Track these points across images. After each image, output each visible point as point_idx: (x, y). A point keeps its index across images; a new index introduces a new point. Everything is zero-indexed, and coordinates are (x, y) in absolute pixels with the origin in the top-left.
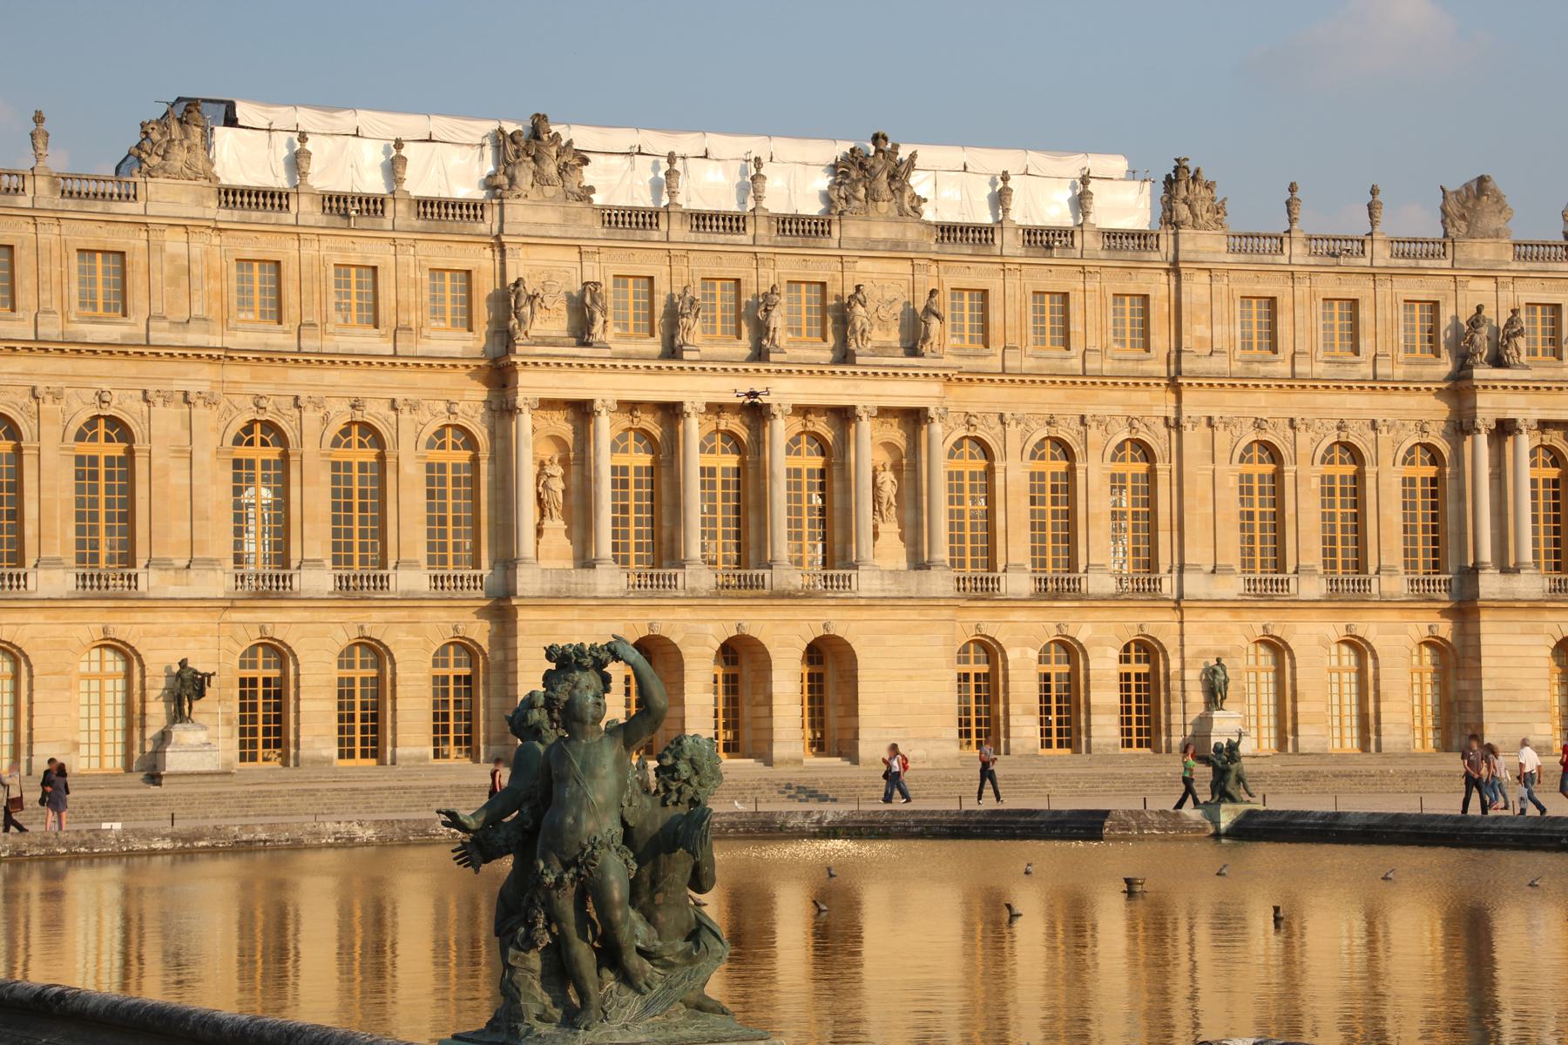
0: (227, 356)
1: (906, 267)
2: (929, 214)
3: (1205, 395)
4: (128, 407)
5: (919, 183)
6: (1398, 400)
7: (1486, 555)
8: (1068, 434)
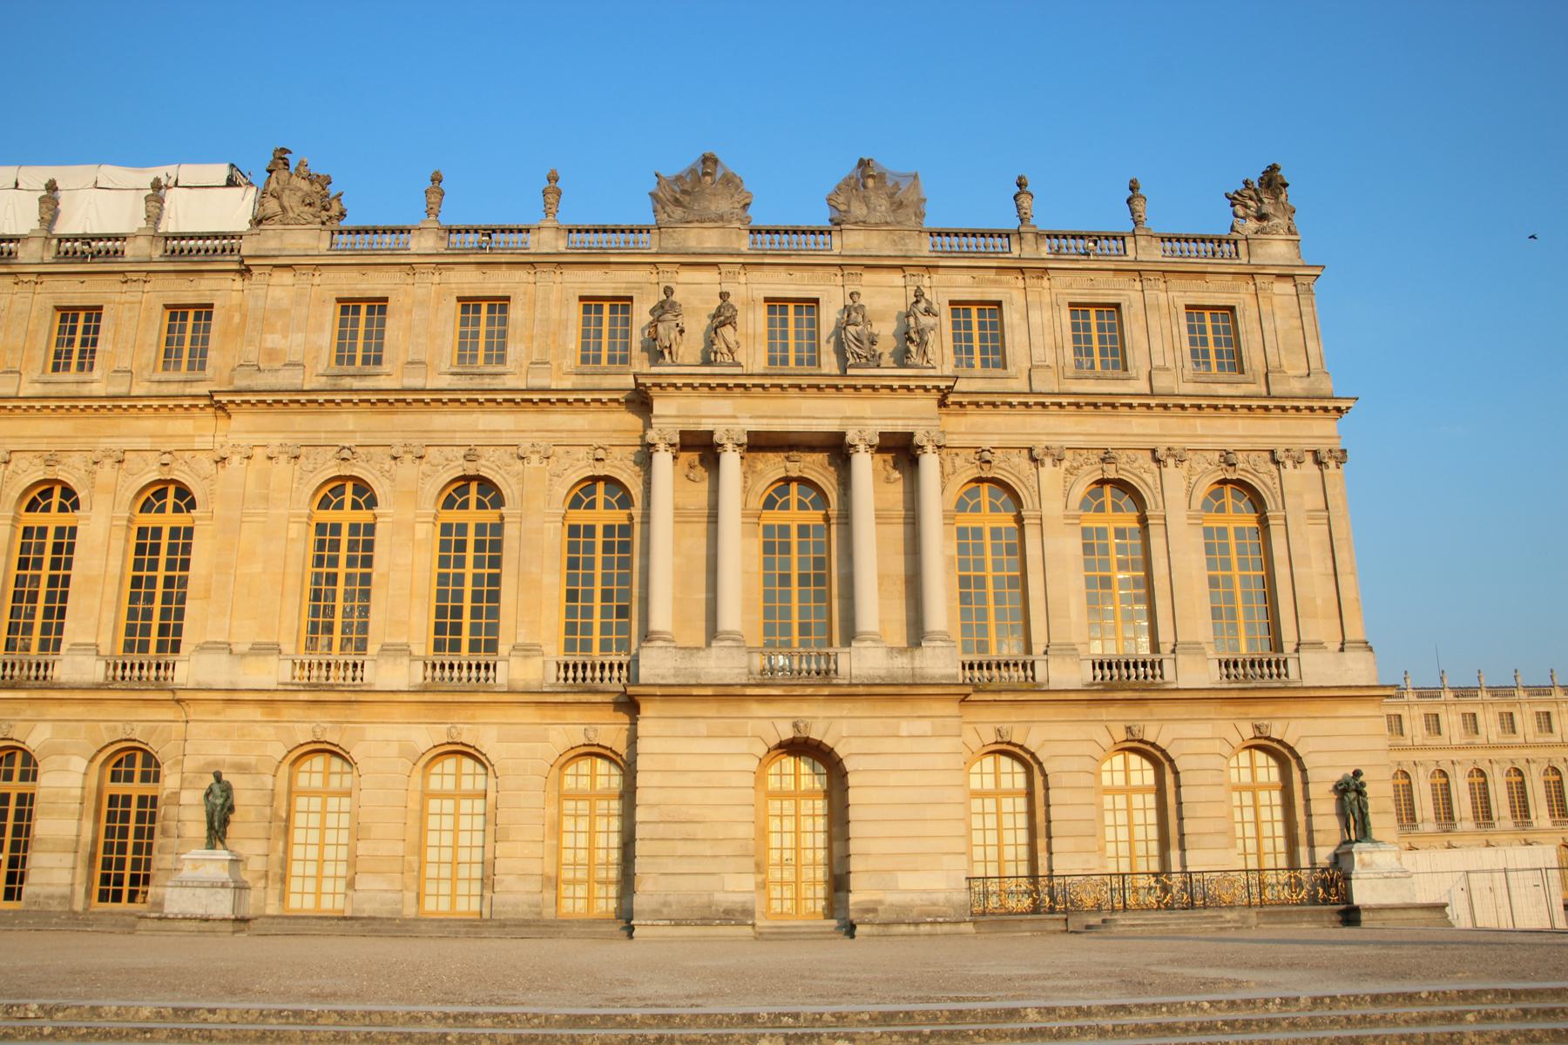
3: (268, 419)
6: (559, 419)
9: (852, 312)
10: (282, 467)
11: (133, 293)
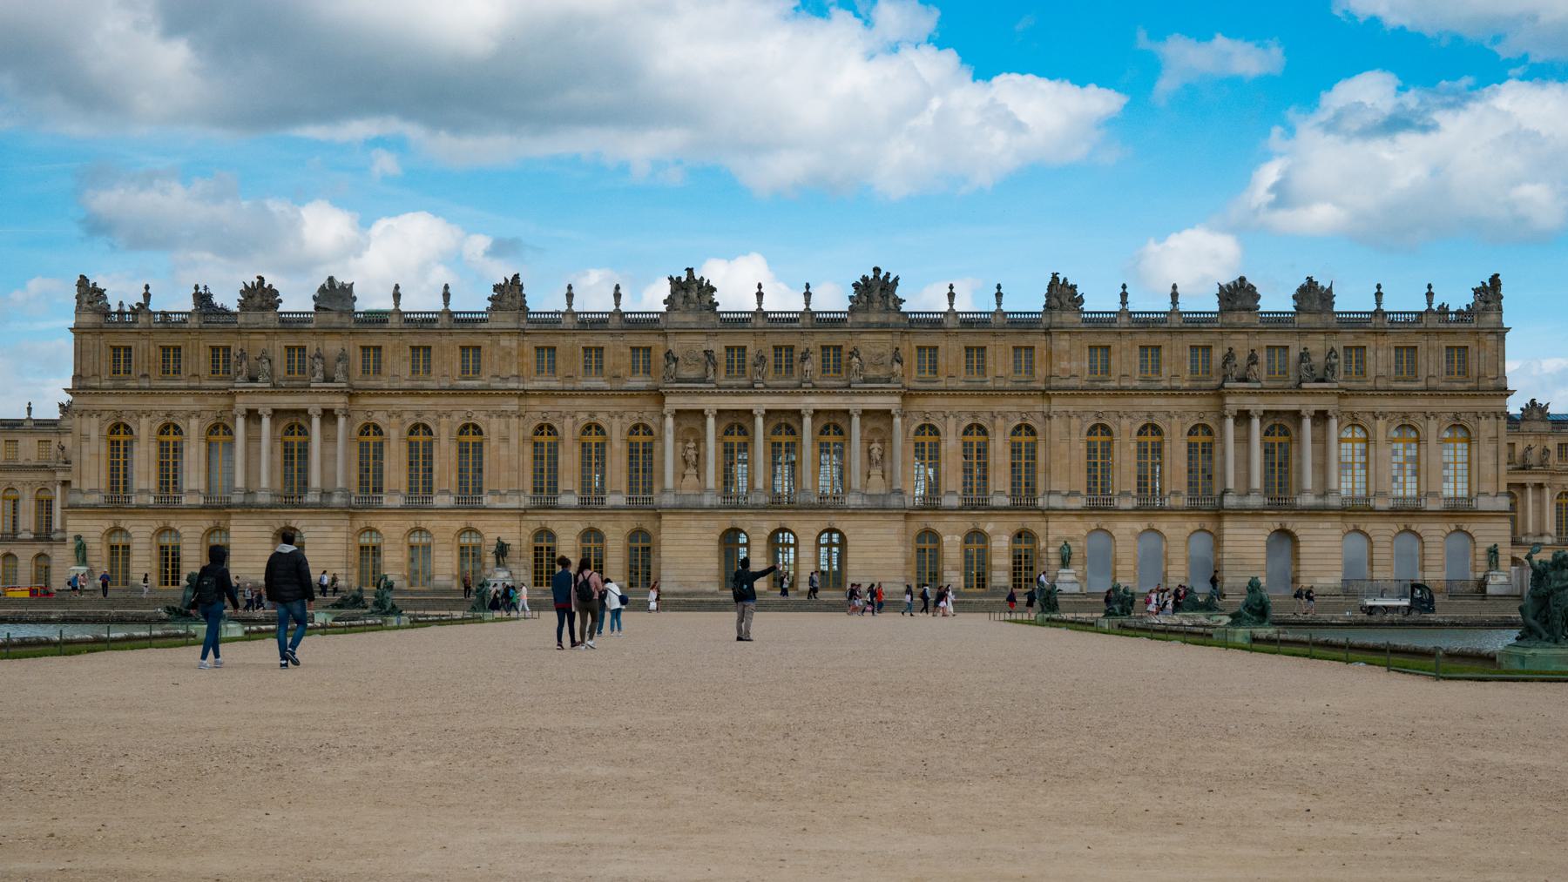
0: (525, 394)
1: (889, 337)
2: (904, 308)
4: (480, 419)
5: (899, 292)
6: (1185, 401)
7: (1231, 485)
9: (1305, 356)
10: (1075, 422)
11: (1000, 341)
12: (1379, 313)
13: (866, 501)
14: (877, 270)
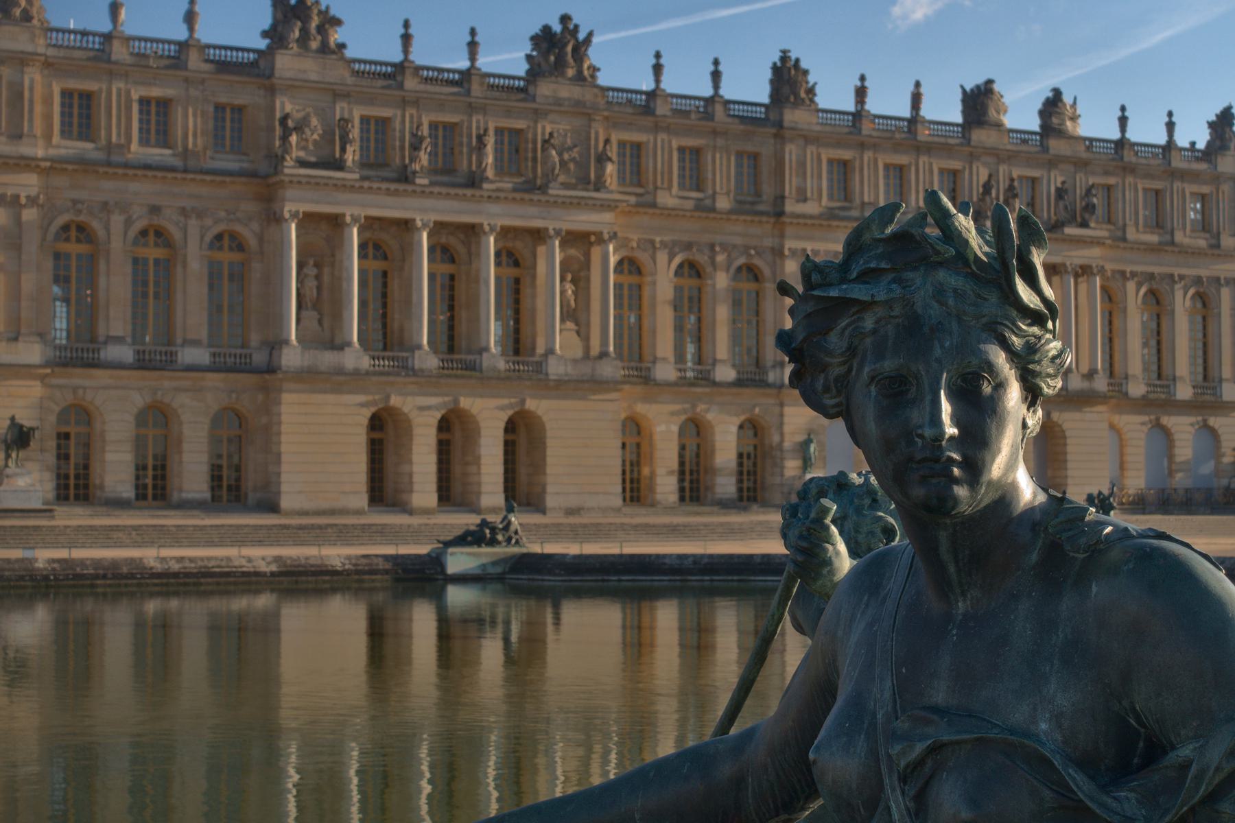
5: (594, 55)
8: (702, 259)
12: (1121, 144)
13: (570, 370)
14: (565, 19)
